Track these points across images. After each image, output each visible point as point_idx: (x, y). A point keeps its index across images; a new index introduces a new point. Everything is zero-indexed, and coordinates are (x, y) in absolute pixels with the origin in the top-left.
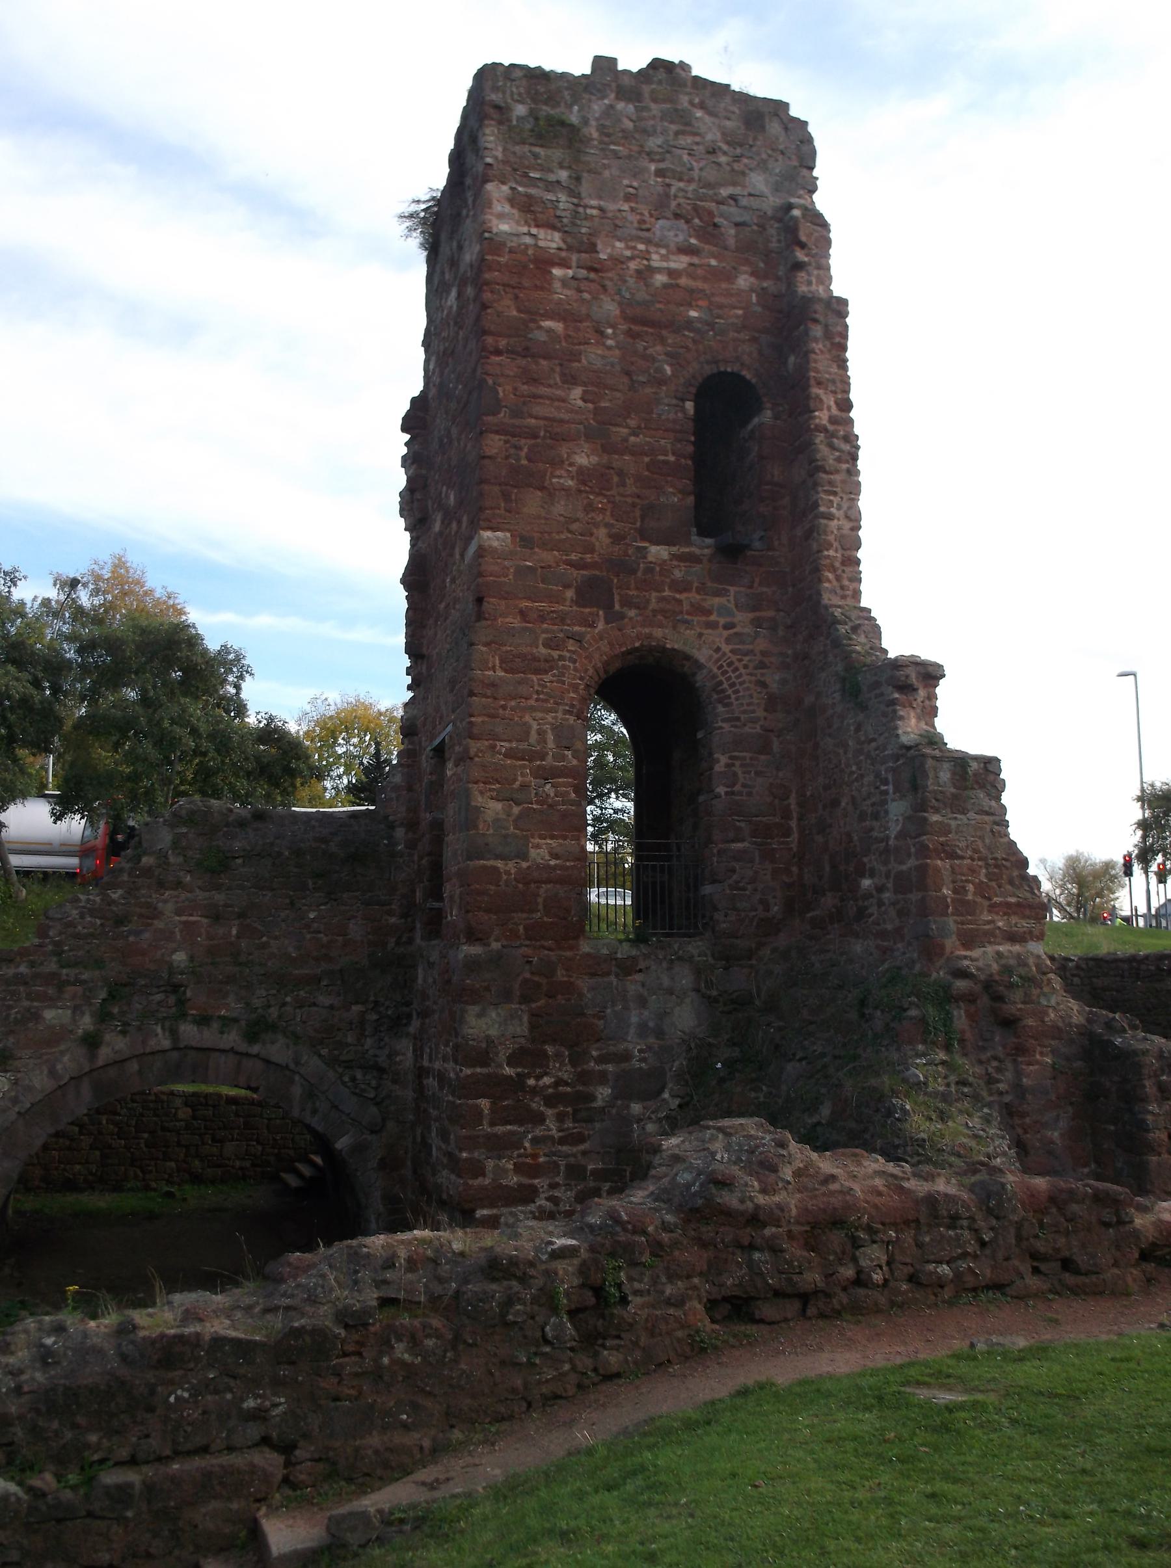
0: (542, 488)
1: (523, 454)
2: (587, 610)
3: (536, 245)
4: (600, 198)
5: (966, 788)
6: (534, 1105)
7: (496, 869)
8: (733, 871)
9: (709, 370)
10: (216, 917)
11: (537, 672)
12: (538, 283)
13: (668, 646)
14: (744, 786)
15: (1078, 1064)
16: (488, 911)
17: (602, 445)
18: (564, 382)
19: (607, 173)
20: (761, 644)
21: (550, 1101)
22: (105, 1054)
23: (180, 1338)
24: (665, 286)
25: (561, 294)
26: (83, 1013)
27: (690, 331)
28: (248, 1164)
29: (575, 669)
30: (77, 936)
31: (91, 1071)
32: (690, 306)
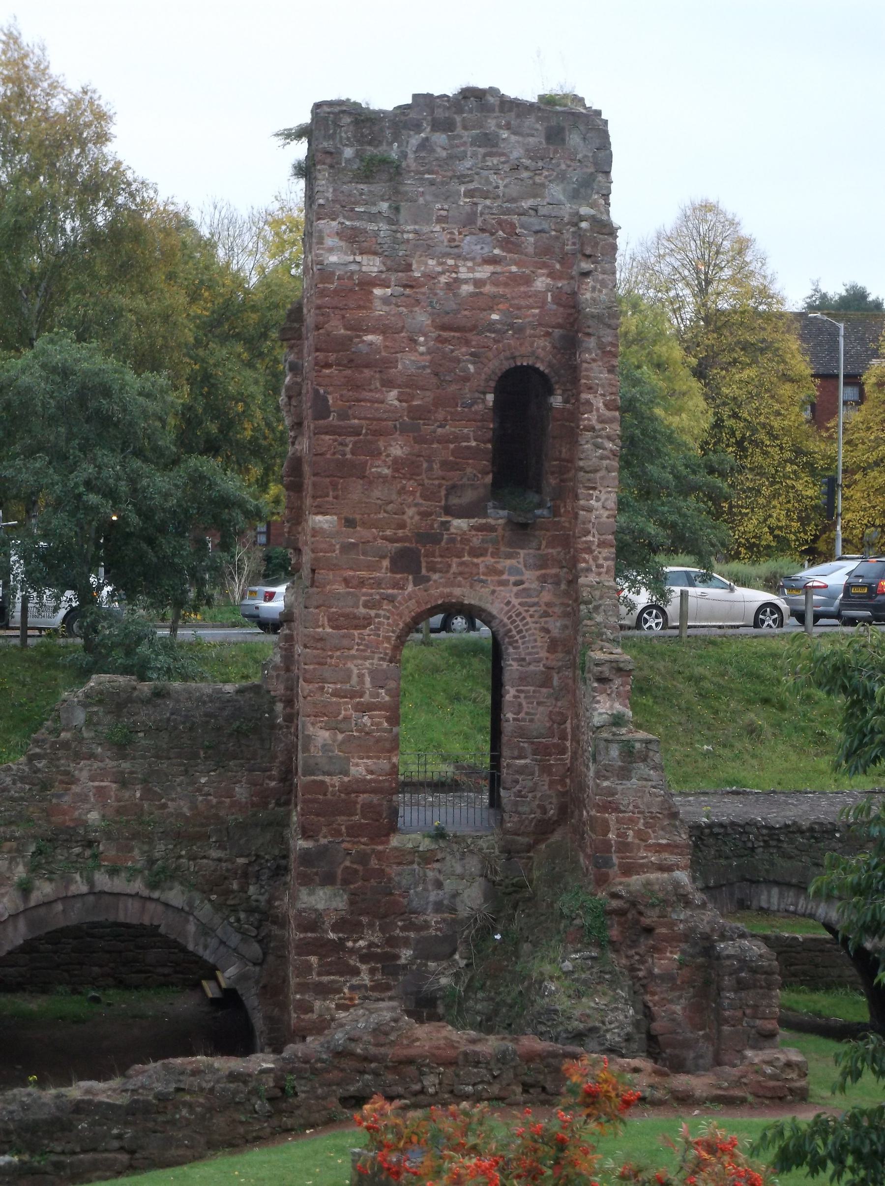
0: (363, 477)
1: (348, 449)
2: (398, 576)
3: (360, 271)
4: (416, 223)
5: (631, 763)
6: (352, 962)
7: (323, 782)
8: (517, 782)
9: (507, 365)
10: (123, 782)
11: (356, 627)
12: (361, 303)
13: (466, 602)
14: (527, 713)
15: (700, 960)
16: (318, 815)
17: (414, 438)
18: (383, 386)
19: (421, 200)
20: (546, 597)
21: (364, 959)
22: (35, 897)
23: (83, 1101)
24: (473, 295)
25: (380, 310)
26: (17, 864)
27: (490, 331)
29: (388, 625)
30: (12, 799)
32: (491, 309)
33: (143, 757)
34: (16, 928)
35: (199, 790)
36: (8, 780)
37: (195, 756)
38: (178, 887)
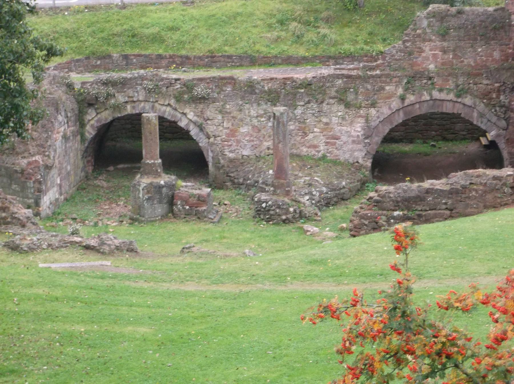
10: (445, 51)
22: (407, 102)
26: (399, 88)
30: (396, 60)
31: (403, 108)
33: (453, 40)
34: (399, 115)
35: (478, 54)
36: (394, 51)
37: (476, 39)
38: (469, 97)
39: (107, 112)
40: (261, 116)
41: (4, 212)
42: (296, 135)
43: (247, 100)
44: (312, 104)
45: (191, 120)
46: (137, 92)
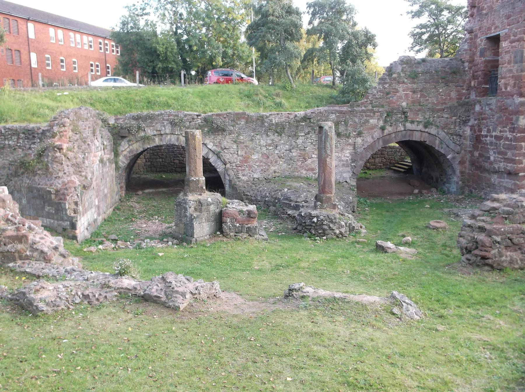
10: (414, 92)
22: (386, 132)
28: (382, 165)
30: (377, 98)
33: (421, 83)
34: (379, 143)
35: (439, 94)
38: (434, 127)
39: (138, 144)
40: (270, 145)
41: (21, 242)
42: (298, 160)
43: (259, 131)
44: (311, 135)
45: (210, 150)
46: (164, 126)
